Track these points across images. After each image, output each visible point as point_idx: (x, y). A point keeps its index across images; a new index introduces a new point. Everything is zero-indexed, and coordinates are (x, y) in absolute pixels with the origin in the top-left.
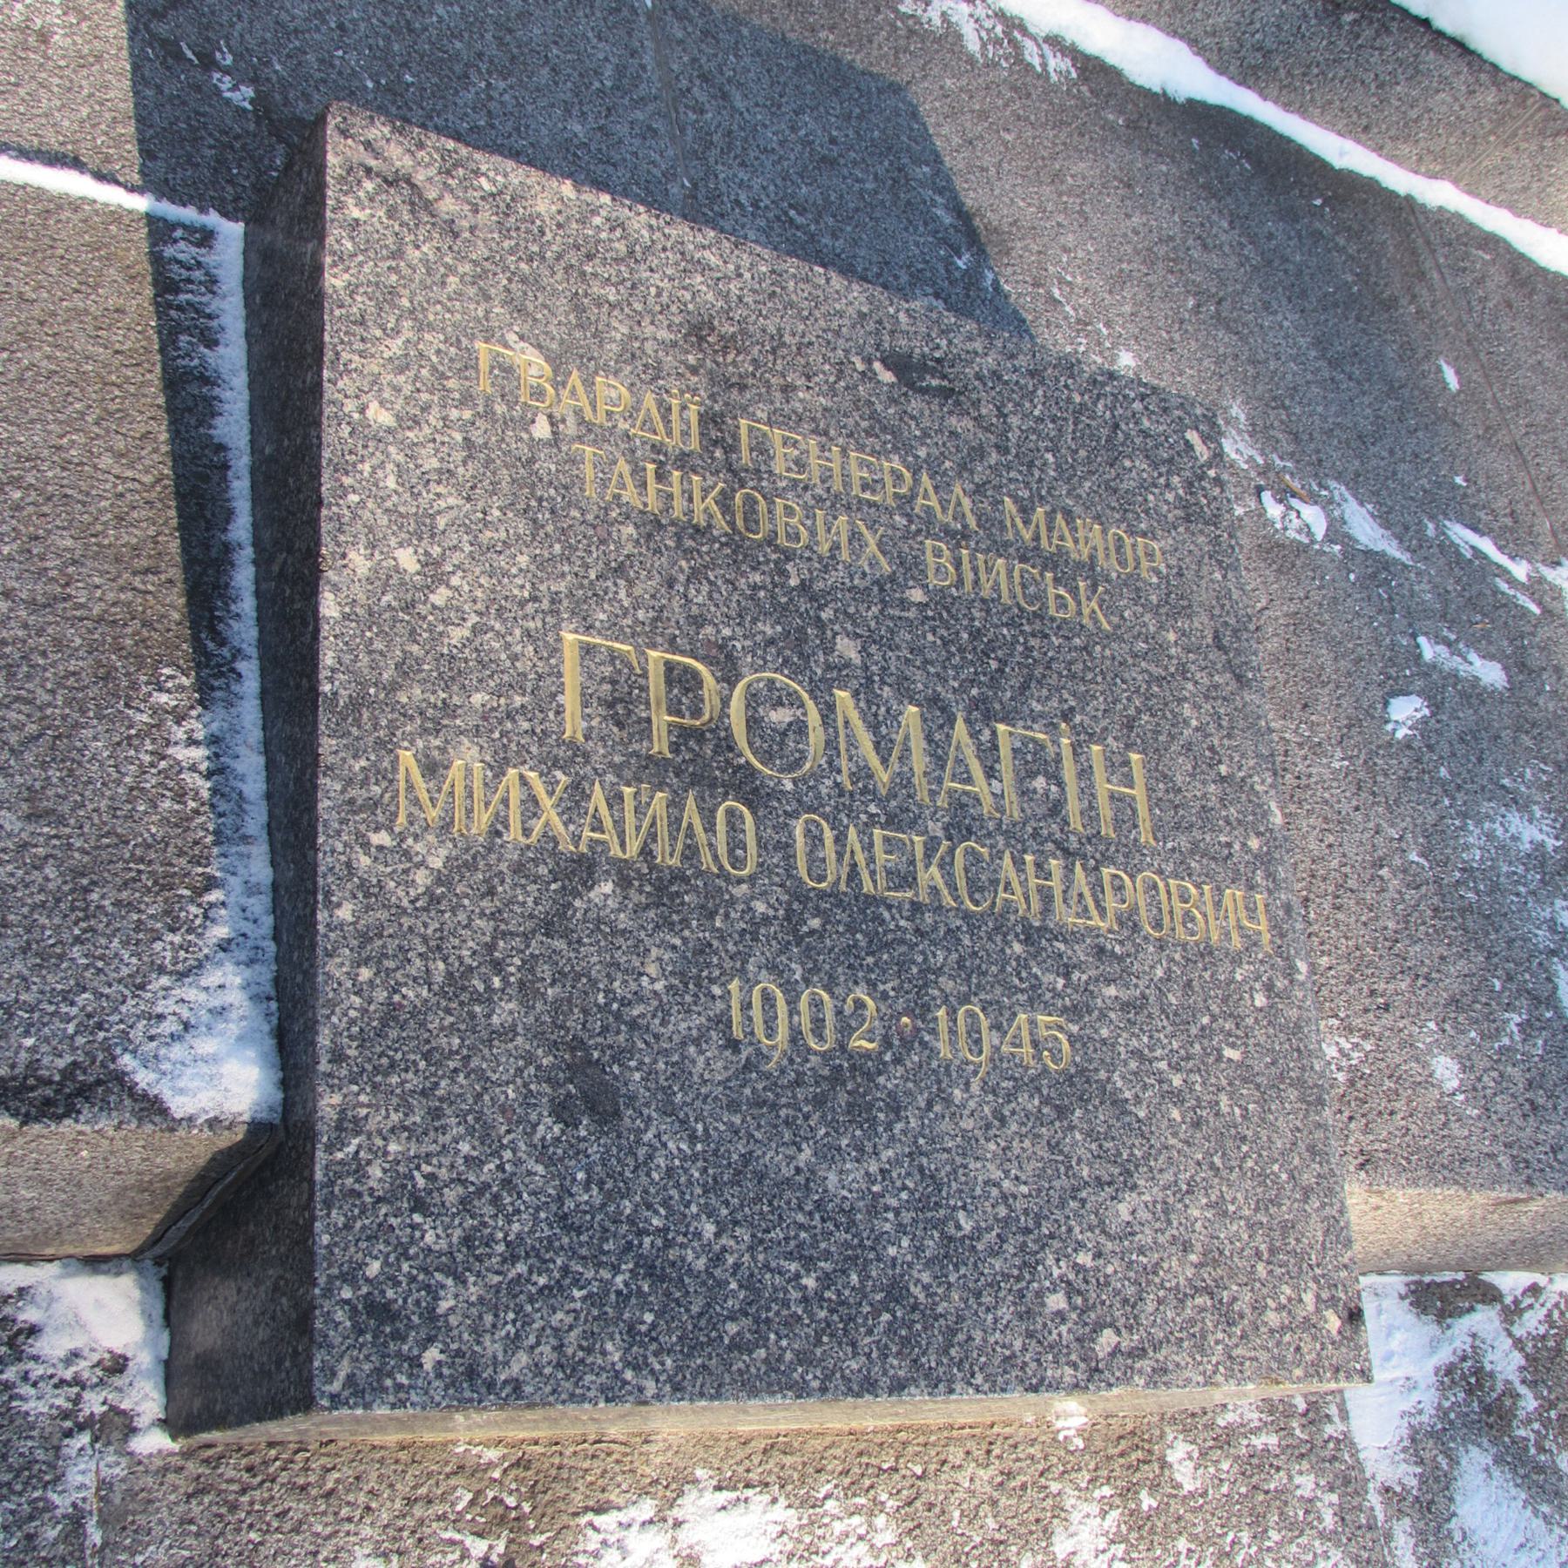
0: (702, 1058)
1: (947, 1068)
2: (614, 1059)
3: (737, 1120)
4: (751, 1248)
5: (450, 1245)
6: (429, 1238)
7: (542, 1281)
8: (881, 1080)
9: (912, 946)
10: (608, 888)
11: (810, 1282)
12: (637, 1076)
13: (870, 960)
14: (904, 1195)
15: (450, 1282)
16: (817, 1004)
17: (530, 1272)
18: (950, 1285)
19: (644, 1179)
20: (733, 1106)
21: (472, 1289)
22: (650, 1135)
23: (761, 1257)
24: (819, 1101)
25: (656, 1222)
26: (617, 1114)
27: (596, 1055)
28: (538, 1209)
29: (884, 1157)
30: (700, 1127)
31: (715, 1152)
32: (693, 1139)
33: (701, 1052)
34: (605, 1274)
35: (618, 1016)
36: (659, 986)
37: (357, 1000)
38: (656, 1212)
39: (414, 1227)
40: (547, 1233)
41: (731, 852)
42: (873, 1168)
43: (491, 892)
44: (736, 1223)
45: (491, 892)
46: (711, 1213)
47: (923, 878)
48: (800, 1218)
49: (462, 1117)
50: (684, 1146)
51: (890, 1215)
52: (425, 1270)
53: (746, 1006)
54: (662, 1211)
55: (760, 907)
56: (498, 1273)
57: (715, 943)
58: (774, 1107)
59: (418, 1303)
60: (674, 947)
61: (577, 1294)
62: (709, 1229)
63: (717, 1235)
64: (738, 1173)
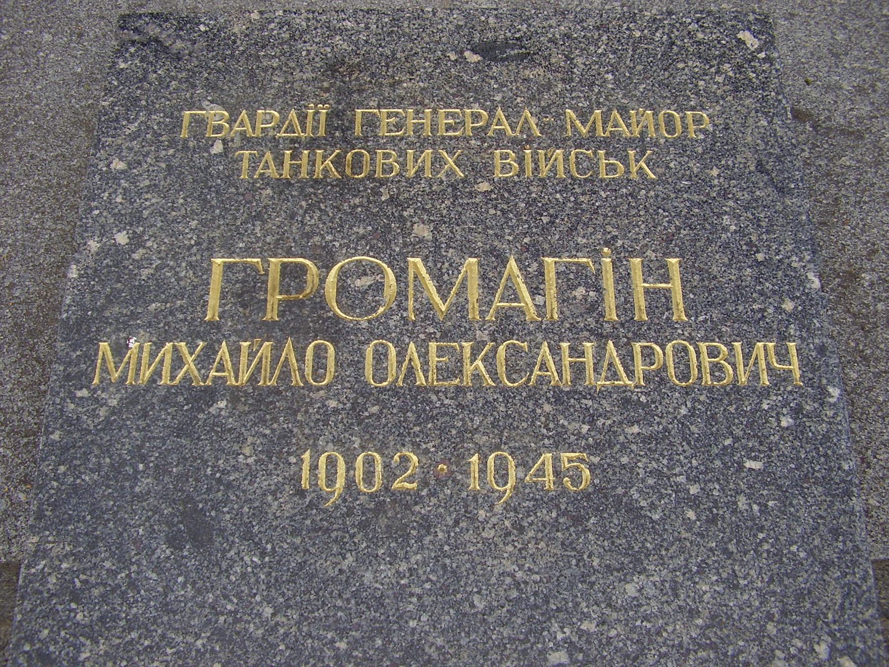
0: (276, 503)
1: (475, 498)
2: (213, 508)
3: (298, 540)
4: (298, 623)
5: (92, 621)
6: (79, 617)
7: (147, 643)
8: (417, 508)
9: (453, 417)
10: (222, 404)
11: (342, 645)
12: (228, 517)
13: (417, 429)
14: (427, 586)
15: (88, 642)
16: (369, 463)
17: (140, 638)
18: (460, 646)
19: (225, 581)
20: (295, 532)
21: (102, 647)
22: (232, 553)
23: (305, 629)
24: (363, 526)
25: (229, 607)
26: (211, 540)
27: (201, 506)
28: (150, 600)
29: (413, 560)
30: (269, 546)
31: (278, 562)
32: (263, 554)
33: (276, 499)
34: (190, 639)
35: (219, 481)
36: (250, 461)
37: (55, 484)
38: (230, 601)
39: (71, 611)
40: (154, 614)
41: (315, 371)
42: (403, 567)
43: (145, 415)
44: (289, 607)
45: (145, 415)
46: (269, 601)
47: (468, 369)
48: (339, 603)
49: (108, 547)
50: (255, 559)
51: (414, 600)
52: (74, 635)
53: (314, 467)
54: (235, 601)
55: (332, 404)
56: (119, 637)
57: (295, 430)
58: (327, 531)
59: (68, 654)
60: (265, 435)
61: (169, 651)
62: (268, 611)
63: (274, 615)
64: (294, 574)
